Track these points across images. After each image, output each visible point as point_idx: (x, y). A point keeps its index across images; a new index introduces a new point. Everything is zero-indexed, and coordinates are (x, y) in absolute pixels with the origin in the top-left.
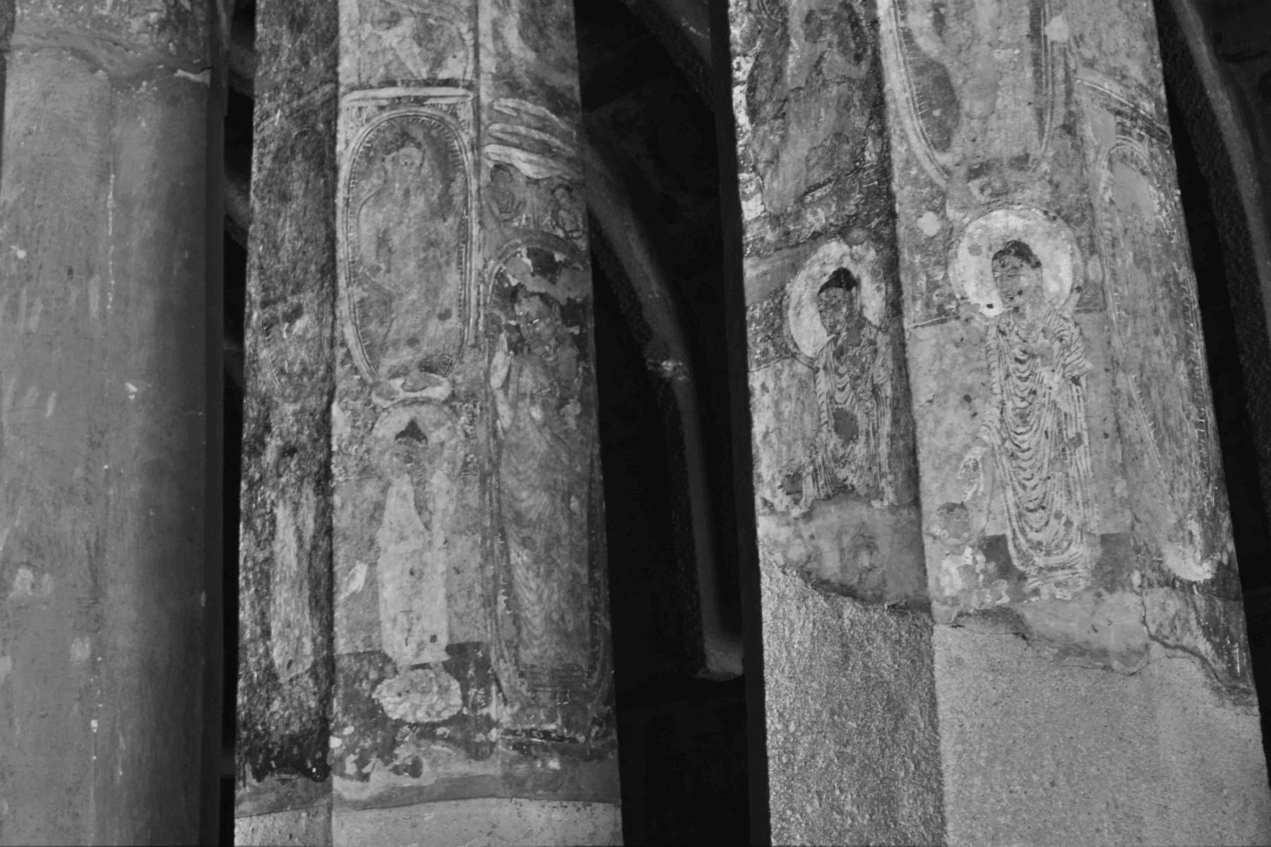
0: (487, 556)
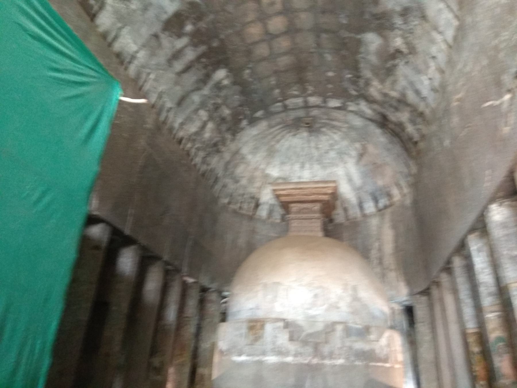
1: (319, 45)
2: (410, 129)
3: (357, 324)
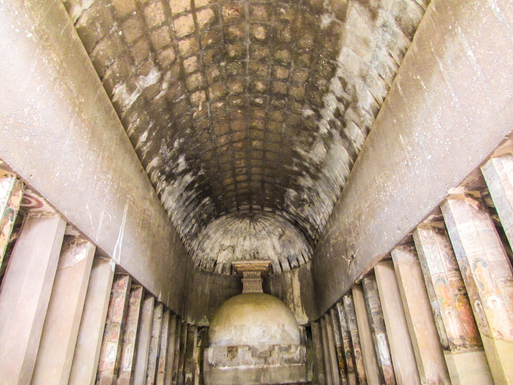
0: (461, 326)
1: (263, 187)
2: (310, 232)
3: (284, 345)
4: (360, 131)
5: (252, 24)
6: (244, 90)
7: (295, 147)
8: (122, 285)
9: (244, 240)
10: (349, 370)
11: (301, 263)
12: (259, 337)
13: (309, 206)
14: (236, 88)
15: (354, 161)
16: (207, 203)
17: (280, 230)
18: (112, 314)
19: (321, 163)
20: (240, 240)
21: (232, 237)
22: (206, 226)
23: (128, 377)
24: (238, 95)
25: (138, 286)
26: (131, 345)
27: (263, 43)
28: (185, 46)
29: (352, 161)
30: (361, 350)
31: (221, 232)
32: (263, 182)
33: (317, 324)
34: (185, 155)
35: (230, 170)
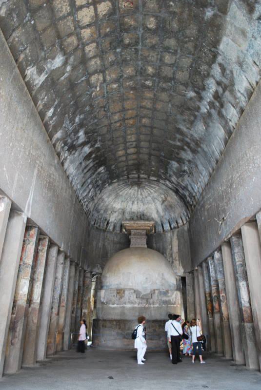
2: (188, 198)
3: (163, 289)
4: (235, 112)
5: (145, 15)
6: (136, 73)
7: (178, 125)
8: (32, 235)
9: (132, 204)
10: (215, 311)
11: (179, 225)
12: (142, 283)
13: (189, 176)
14: (129, 71)
15: (229, 137)
16: (102, 171)
17: (163, 196)
18: (24, 257)
19: (201, 139)
20: (129, 204)
21: (122, 201)
22: (101, 191)
23: (37, 307)
24: (130, 78)
25: (45, 237)
26: (40, 283)
27: (154, 32)
28: (86, 33)
29: (227, 138)
30: (226, 295)
31: (113, 197)
32: (150, 155)
33: (191, 275)
34: (84, 129)
35: (123, 143)
